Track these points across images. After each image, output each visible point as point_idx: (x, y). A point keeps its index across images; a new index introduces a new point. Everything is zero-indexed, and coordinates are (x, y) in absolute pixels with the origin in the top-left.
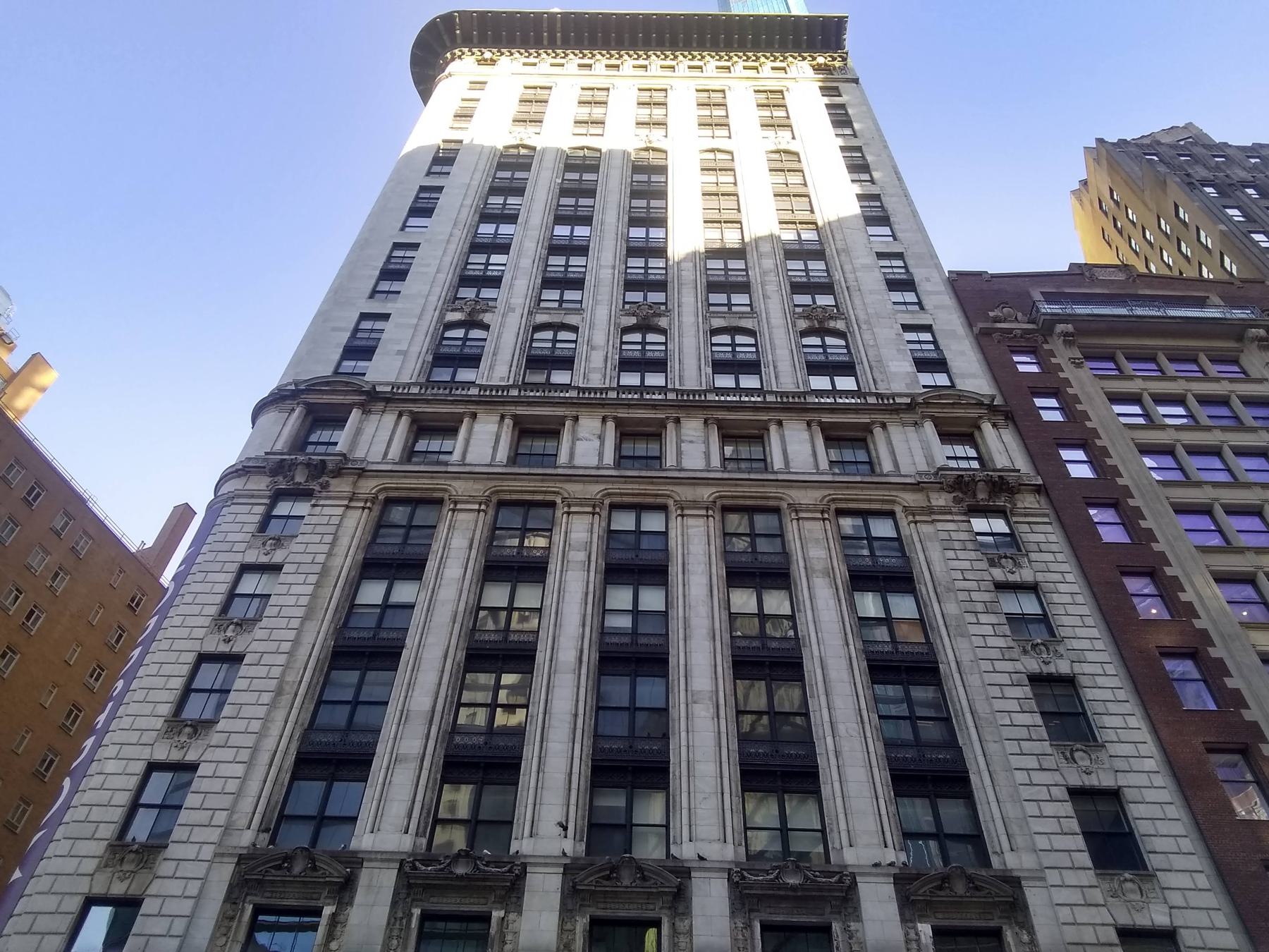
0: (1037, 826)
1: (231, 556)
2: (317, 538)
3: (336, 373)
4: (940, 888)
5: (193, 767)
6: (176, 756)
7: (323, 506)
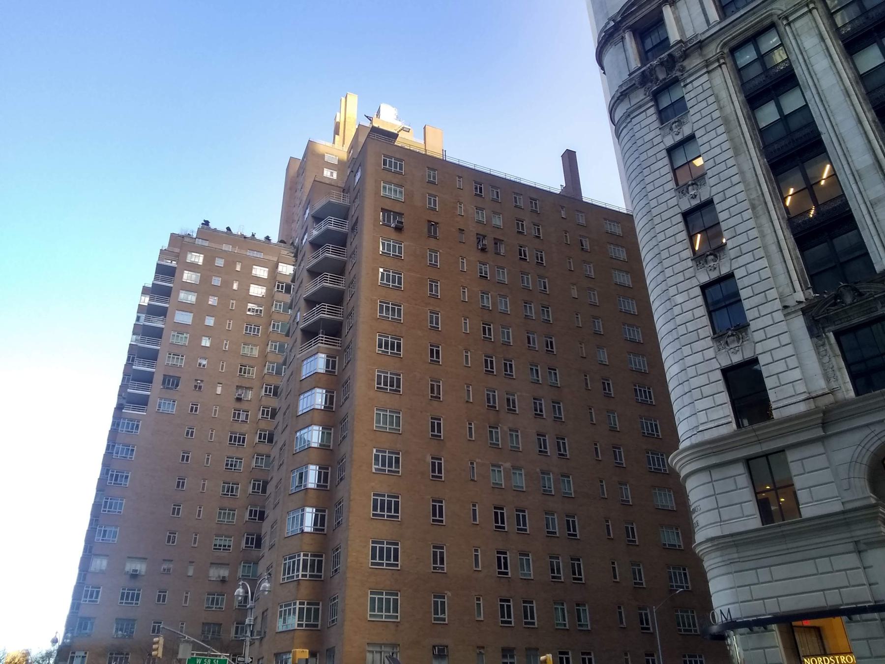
1: (657, 149)
2: (704, 104)
6: (714, 275)
7: (691, 82)
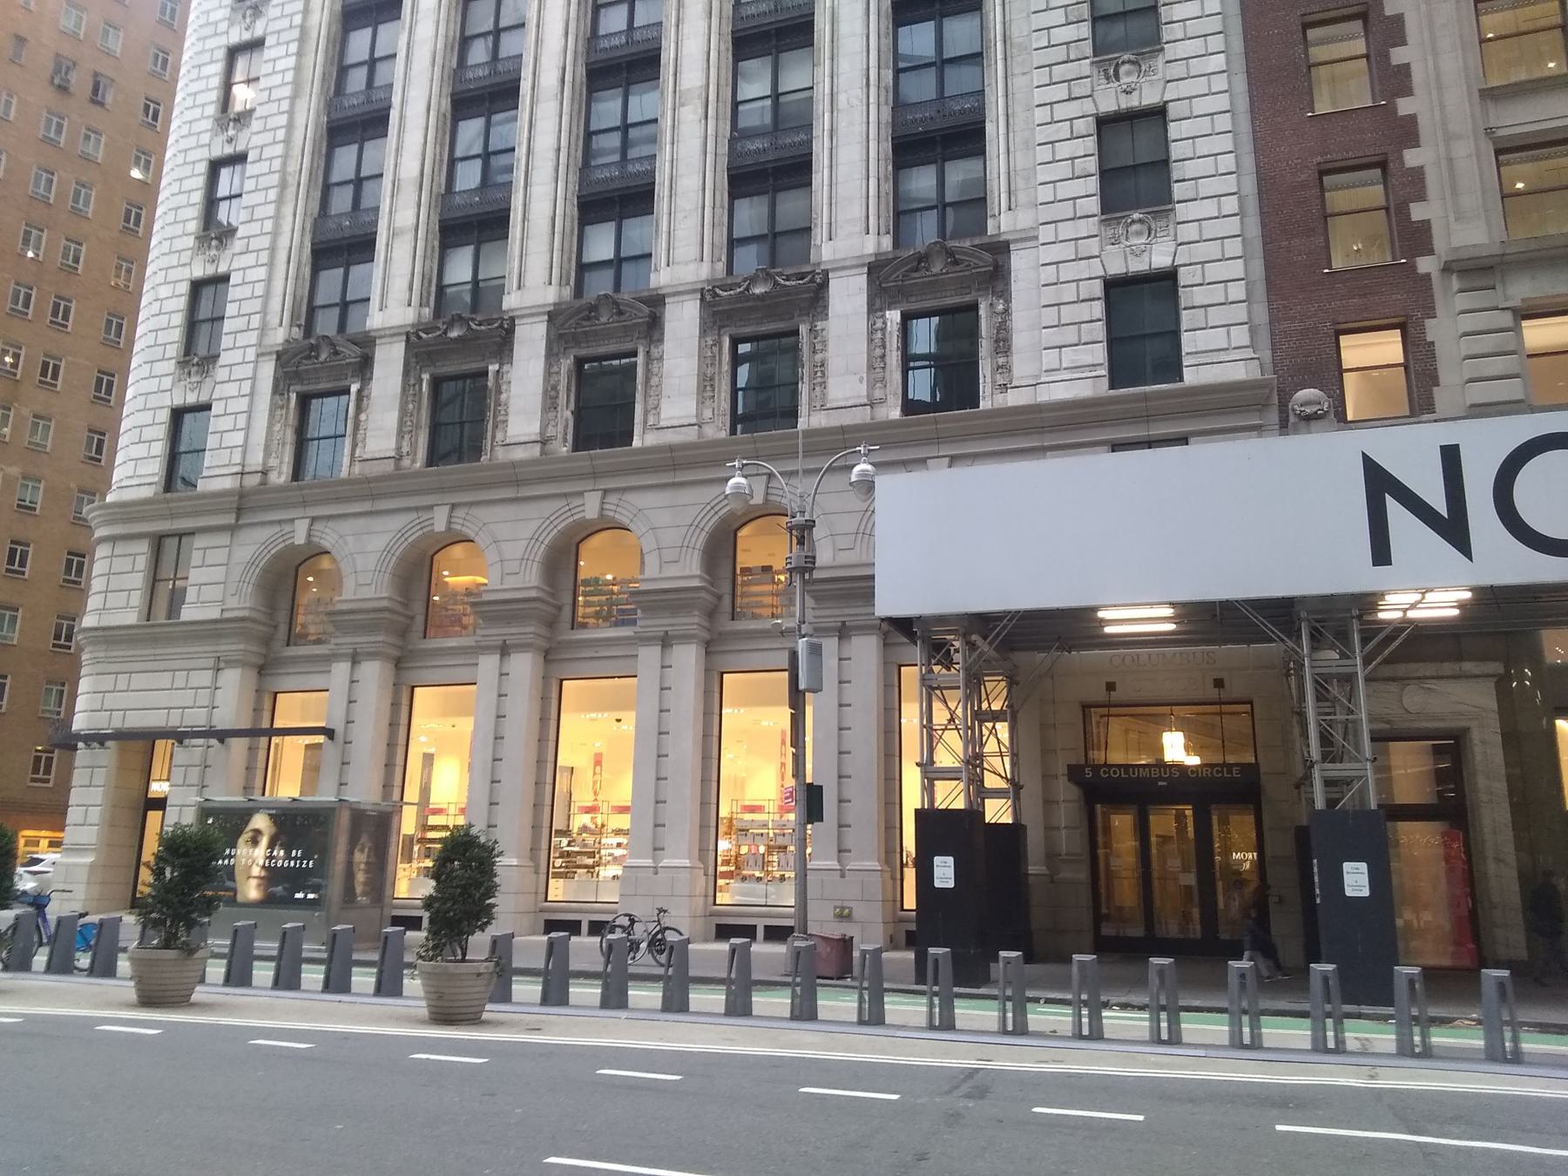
0: (1044, 174)
4: (916, 270)
5: (224, 279)
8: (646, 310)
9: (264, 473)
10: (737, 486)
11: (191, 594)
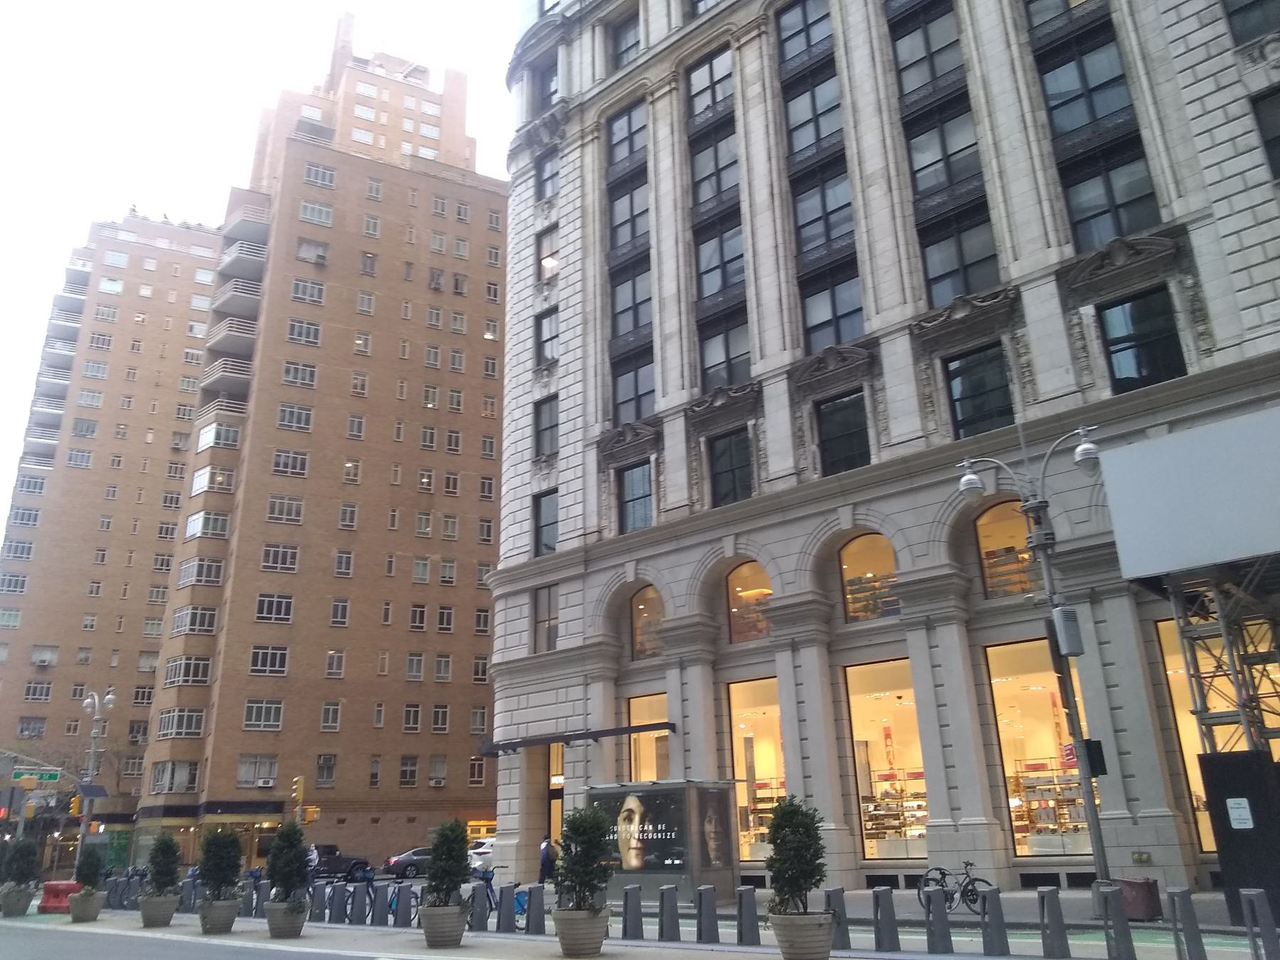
0: (1206, 159)
3: (543, 13)
4: (1102, 267)
5: (554, 397)
8: (864, 352)
9: (599, 532)
10: (970, 482)
11: (562, 630)
